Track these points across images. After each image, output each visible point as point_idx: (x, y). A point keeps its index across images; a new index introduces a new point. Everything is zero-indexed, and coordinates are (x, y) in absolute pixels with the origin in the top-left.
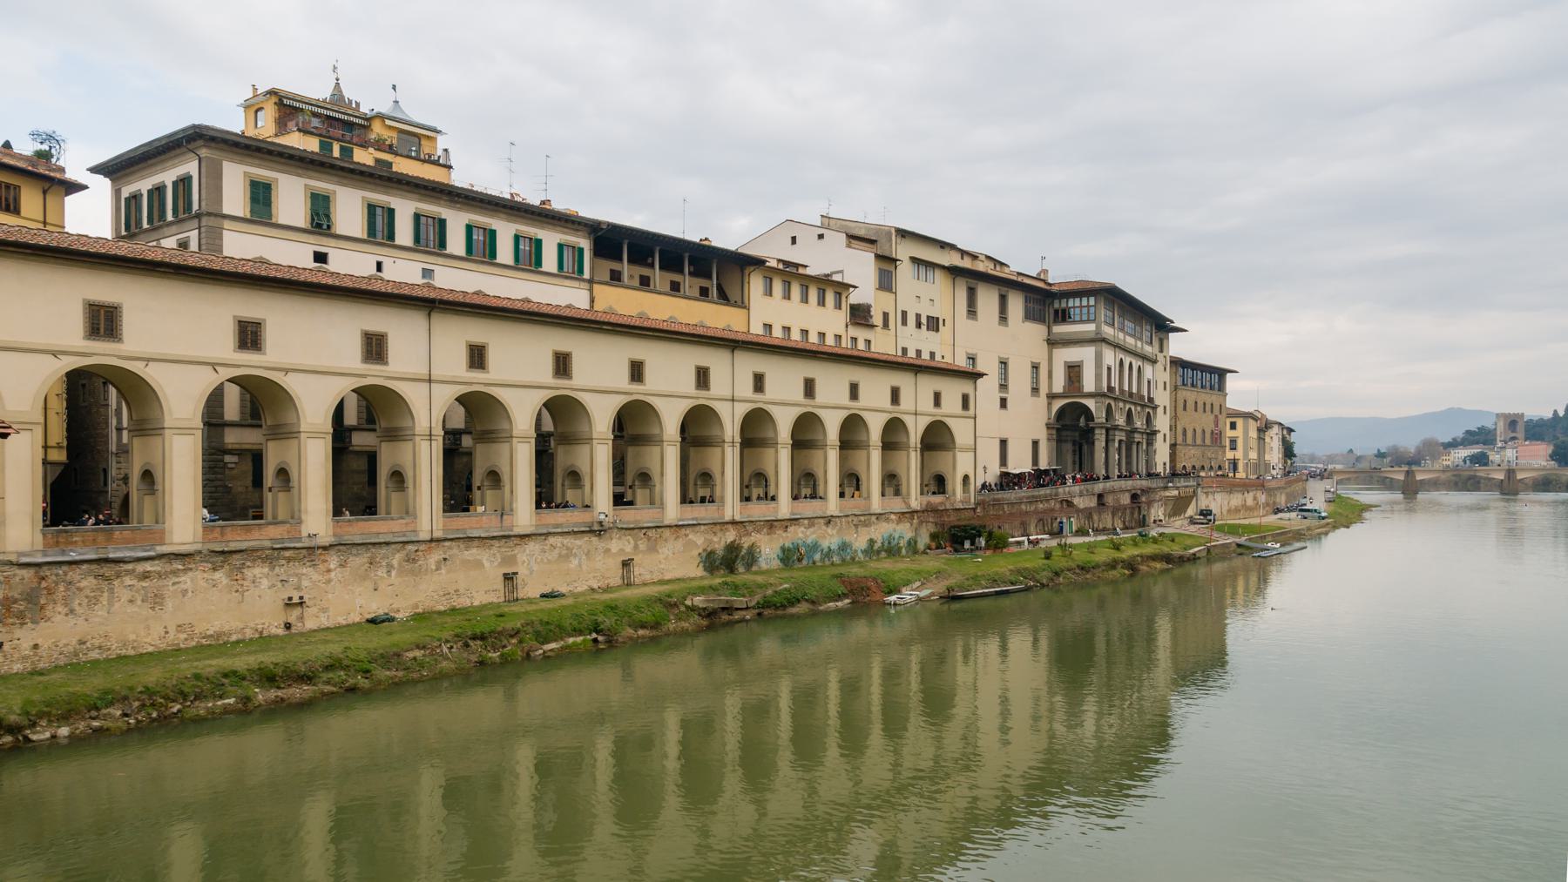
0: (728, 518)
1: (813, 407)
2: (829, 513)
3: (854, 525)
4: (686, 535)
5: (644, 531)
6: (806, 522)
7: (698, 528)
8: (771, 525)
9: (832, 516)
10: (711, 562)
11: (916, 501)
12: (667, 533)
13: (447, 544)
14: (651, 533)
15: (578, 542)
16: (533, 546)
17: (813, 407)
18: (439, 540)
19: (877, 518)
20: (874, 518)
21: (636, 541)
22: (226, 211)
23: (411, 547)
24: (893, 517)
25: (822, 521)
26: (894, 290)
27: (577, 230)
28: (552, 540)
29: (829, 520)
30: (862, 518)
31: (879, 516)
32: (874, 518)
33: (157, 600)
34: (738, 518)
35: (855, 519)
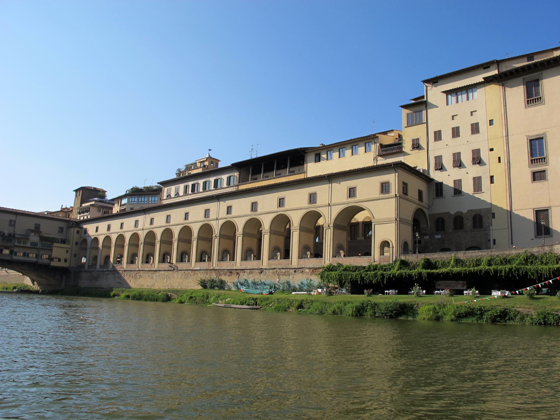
0: (212, 268)
1: (255, 215)
2: (261, 267)
3: (277, 275)
4: (197, 274)
5: (184, 271)
6: (248, 271)
7: (201, 271)
8: (231, 272)
9: (262, 269)
10: (204, 285)
11: (328, 259)
12: (190, 271)
13: (142, 272)
14: (186, 272)
15: (167, 274)
16: (158, 273)
17: (255, 215)
18: (140, 271)
19: (295, 271)
20: (292, 271)
21: (182, 275)
22: (164, 199)
23: (136, 272)
24: (307, 270)
25: (257, 271)
26: (425, 121)
27: (233, 170)
28: (161, 272)
29: (261, 271)
30: (283, 271)
31: (296, 270)
32: (292, 271)
33: (107, 279)
34: (216, 268)
35: (278, 271)
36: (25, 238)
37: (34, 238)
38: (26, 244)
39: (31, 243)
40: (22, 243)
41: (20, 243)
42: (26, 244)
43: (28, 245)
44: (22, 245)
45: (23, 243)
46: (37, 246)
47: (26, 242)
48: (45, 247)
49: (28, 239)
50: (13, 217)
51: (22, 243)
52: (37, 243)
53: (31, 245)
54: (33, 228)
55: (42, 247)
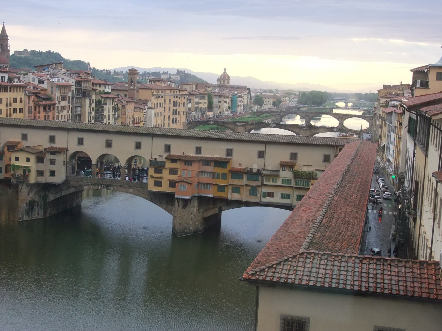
36: (274, 175)
37: (287, 174)
38: (276, 182)
39: (283, 180)
40: (271, 180)
41: (269, 181)
42: (276, 182)
43: (279, 183)
44: (271, 183)
45: (273, 182)
46: (291, 184)
47: (276, 179)
48: (301, 185)
49: (278, 176)
50: (261, 148)
51: (271, 180)
52: (291, 180)
53: (282, 183)
54: (287, 159)
55: (296, 185)
